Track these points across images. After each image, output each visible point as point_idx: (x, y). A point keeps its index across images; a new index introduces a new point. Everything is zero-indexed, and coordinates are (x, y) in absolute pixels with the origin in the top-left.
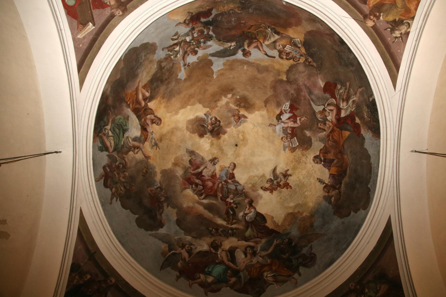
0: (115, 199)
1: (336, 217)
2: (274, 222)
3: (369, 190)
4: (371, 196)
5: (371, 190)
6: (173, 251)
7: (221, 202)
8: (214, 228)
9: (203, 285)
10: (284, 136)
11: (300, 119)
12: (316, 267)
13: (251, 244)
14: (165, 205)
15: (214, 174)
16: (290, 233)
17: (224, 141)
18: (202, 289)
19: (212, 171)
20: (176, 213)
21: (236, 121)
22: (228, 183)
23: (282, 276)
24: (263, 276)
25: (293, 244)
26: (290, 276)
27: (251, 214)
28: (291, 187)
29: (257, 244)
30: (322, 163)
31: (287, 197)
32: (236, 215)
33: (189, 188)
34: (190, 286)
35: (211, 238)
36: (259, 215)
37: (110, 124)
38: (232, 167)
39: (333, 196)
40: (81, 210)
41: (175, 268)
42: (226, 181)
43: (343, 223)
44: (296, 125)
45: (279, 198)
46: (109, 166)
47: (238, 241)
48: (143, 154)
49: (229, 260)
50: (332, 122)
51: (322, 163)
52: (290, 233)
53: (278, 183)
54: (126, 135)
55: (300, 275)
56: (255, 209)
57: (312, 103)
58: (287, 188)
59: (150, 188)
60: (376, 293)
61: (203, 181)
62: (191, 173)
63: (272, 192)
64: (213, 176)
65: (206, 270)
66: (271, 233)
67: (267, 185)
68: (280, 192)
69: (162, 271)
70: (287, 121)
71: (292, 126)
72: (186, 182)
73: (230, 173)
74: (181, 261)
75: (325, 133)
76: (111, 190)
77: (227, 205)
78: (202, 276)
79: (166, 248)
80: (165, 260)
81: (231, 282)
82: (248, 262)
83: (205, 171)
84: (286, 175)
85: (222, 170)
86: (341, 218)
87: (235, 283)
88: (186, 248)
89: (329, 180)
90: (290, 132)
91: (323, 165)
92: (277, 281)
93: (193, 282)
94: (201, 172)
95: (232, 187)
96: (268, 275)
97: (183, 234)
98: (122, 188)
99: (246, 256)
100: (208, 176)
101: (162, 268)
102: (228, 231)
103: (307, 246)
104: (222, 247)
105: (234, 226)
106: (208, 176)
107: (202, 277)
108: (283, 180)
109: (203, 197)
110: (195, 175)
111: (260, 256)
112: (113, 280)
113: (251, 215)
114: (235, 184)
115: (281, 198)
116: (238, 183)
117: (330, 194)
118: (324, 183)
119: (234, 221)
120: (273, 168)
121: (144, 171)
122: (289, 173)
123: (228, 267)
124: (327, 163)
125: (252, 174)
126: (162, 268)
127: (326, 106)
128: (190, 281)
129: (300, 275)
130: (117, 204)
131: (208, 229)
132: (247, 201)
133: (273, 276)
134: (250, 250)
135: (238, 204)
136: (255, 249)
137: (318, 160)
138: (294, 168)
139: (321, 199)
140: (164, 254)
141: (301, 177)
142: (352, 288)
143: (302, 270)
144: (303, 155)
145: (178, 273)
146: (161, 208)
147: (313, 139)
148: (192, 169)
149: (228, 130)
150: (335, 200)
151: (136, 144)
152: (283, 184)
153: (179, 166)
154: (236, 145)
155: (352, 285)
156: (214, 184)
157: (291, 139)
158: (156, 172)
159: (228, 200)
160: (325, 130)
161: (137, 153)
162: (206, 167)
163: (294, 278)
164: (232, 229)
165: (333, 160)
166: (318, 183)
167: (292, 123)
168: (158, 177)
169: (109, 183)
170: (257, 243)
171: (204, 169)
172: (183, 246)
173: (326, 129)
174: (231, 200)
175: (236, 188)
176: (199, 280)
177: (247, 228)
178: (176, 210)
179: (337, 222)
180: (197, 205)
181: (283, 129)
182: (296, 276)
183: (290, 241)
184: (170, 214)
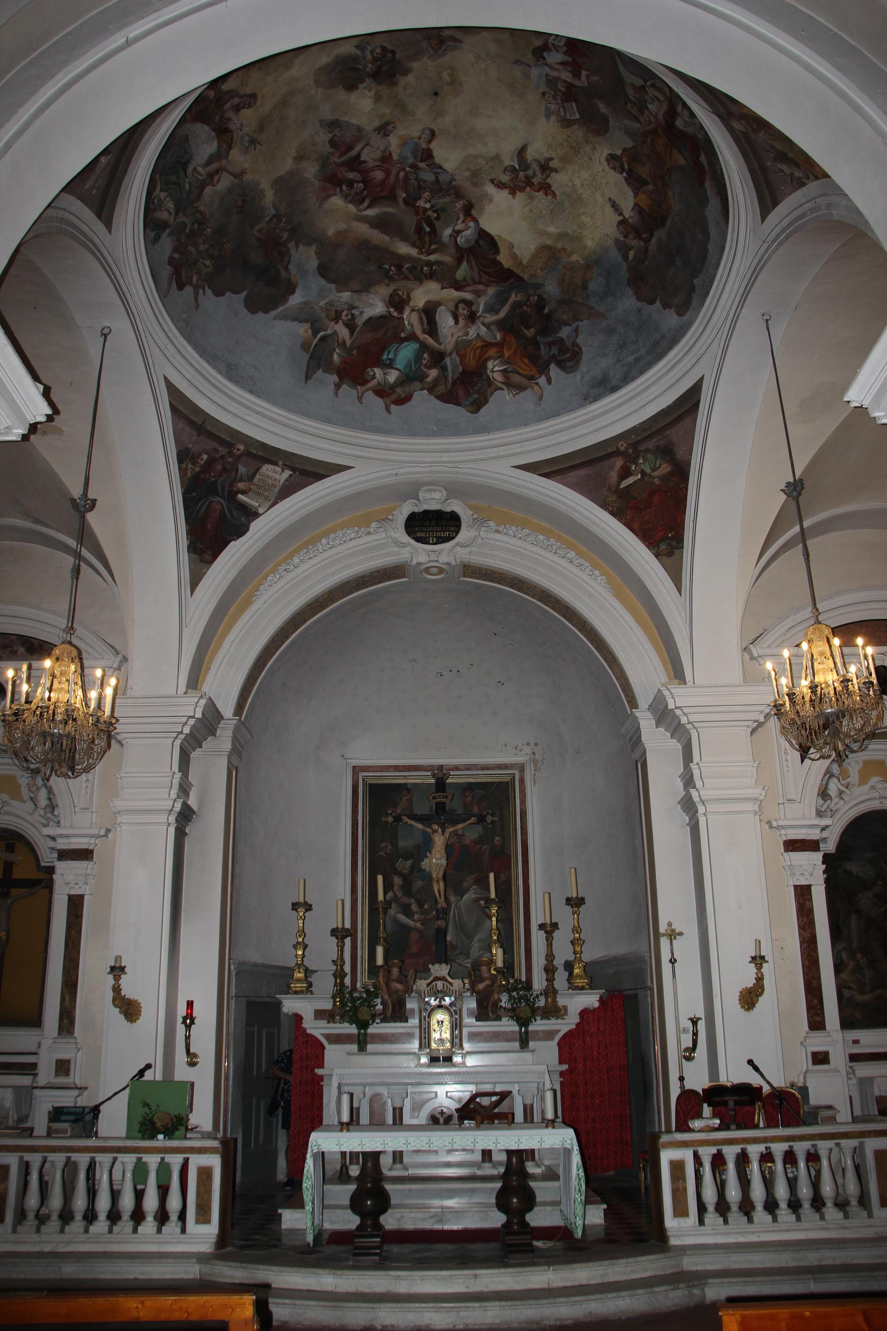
0: (201, 291)
1: (629, 291)
2: (514, 256)
3: (692, 289)
4: (695, 302)
5: (697, 292)
6: (322, 334)
7: (405, 208)
8: (392, 264)
9: (381, 392)
10: (548, 90)
11: (588, 76)
12: (578, 376)
13: (467, 296)
14: (291, 245)
15: (387, 154)
16: (543, 285)
17: (405, 88)
18: (380, 402)
19: (382, 148)
20: (317, 253)
21: (432, 48)
22: (419, 168)
23: (520, 374)
24: (486, 368)
25: (546, 311)
26: (532, 378)
27: (468, 232)
28: (554, 193)
29: (479, 296)
30: (624, 174)
31: (544, 212)
32: (436, 234)
33: (335, 195)
34: (360, 399)
35: (388, 285)
36: (483, 235)
37: (159, 182)
38: (426, 136)
39: (633, 247)
40: (165, 378)
41: (329, 367)
42: (414, 166)
43: (639, 310)
44: (576, 82)
45: (528, 208)
46: (175, 250)
47: (442, 288)
48: (231, 174)
49: (424, 332)
50: (656, 117)
51: (624, 174)
52: (543, 285)
53: (527, 177)
54: (189, 171)
55: (549, 381)
56: (476, 221)
57: (619, 61)
58: (546, 194)
59: (257, 228)
60: (654, 470)
61: (364, 173)
62: (335, 162)
63: (513, 193)
64: (386, 158)
65: (385, 357)
66: (506, 277)
67: (505, 178)
68: (531, 198)
69: (309, 382)
70: (557, 66)
71: (568, 80)
72: (328, 185)
73: (423, 149)
74: (337, 350)
75: (639, 125)
76: (191, 285)
77: (417, 214)
78: (378, 372)
79: (306, 332)
80: (311, 358)
81: (429, 379)
82: (460, 334)
83: (365, 151)
84: (546, 167)
85: (404, 143)
86: (638, 299)
87: (436, 381)
88: (344, 318)
89: (632, 214)
90: (564, 90)
91: (626, 180)
92: (509, 384)
93: (364, 388)
94: (359, 155)
95: (428, 176)
96: (495, 368)
97: (335, 291)
98: (208, 262)
99: (457, 322)
100: (375, 160)
101: (308, 377)
102: (422, 268)
103: (570, 325)
104: (411, 304)
105: (433, 258)
106: (375, 160)
107: (377, 375)
108: (540, 175)
109: (366, 204)
110: (346, 167)
111: (483, 324)
112: (242, 447)
113: (468, 235)
114: (435, 170)
115: (531, 211)
116: (441, 168)
117: (628, 241)
118: (621, 214)
119: (433, 247)
120: (520, 146)
121: (240, 203)
122: (552, 164)
123: (424, 347)
124: (635, 182)
125: (471, 151)
126: (308, 377)
127: (648, 84)
128: (359, 387)
129: (549, 381)
130: (208, 299)
131: (380, 267)
132: (459, 204)
133: (504, 370)
134: (464, 309)
135: (441, 212)
136: (474, 308)
137: (617, 165)
138: (565, 160)
139: (610, 242)
140: (305, 346)
141: (578, 183)
142: (622, 449)
143: (554, 370)
144: (587, 142)
145: (335, 378)
146: (284, 255)
147: (612, 122)
148: (337, 155)
149: (415, 65)
150: (634, 258)
151: (213, 167)
152: (539, 183)
153: (309, 159)
154: (436, 94)
155: (622, 446)
156: (388, 173)
157: (563, 102)
158: (262, 191)
159: (421, 203)
160: (639, 121)
161: (218, 181)
162: (368, 144)
163: (537, 384)
164: (430, 264)
165: (647, 183)
166: (609, 209)
167: (568, 74)
168: (269, 196)
169: (184, 278)
170: (478, 294)
171: (363, 148)
172: (337, 318)
173: (642, 121)
174: (426, 203)
175: (437, 178)
176: (374, 383)
177: (459, 261)
178: (314, 247)
179: (628, 302)
180: (355, 224)
181: (547, 79)
182: (542, 380)
183: (541, 304)
184: (305, 258)
